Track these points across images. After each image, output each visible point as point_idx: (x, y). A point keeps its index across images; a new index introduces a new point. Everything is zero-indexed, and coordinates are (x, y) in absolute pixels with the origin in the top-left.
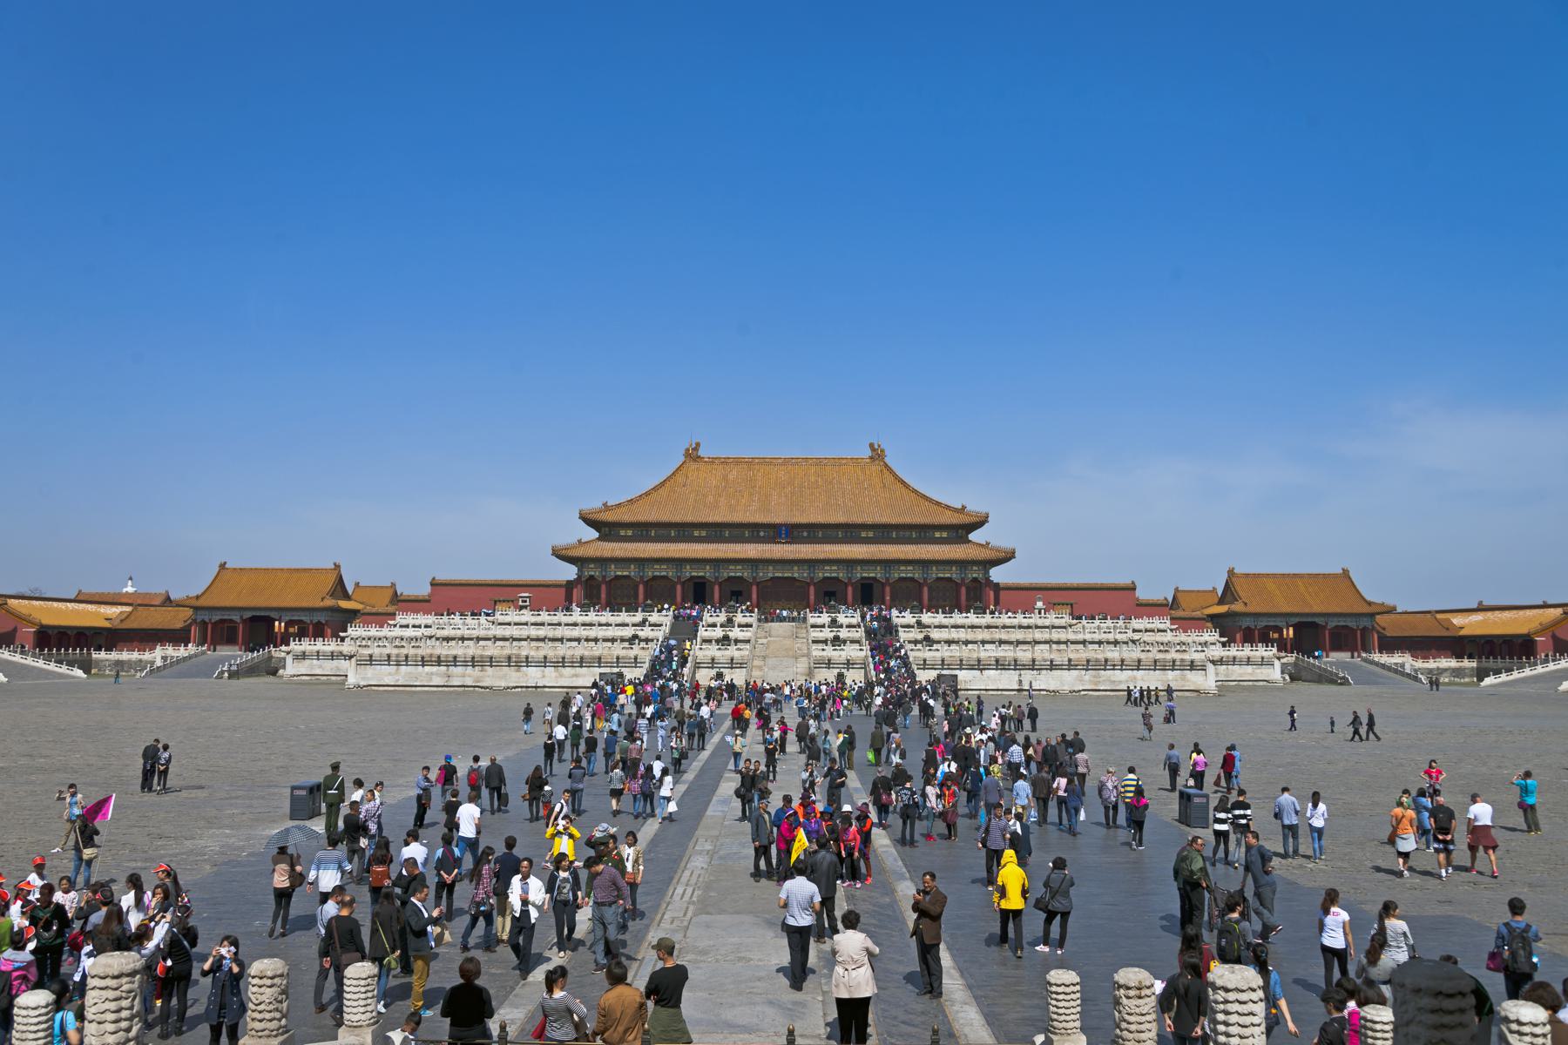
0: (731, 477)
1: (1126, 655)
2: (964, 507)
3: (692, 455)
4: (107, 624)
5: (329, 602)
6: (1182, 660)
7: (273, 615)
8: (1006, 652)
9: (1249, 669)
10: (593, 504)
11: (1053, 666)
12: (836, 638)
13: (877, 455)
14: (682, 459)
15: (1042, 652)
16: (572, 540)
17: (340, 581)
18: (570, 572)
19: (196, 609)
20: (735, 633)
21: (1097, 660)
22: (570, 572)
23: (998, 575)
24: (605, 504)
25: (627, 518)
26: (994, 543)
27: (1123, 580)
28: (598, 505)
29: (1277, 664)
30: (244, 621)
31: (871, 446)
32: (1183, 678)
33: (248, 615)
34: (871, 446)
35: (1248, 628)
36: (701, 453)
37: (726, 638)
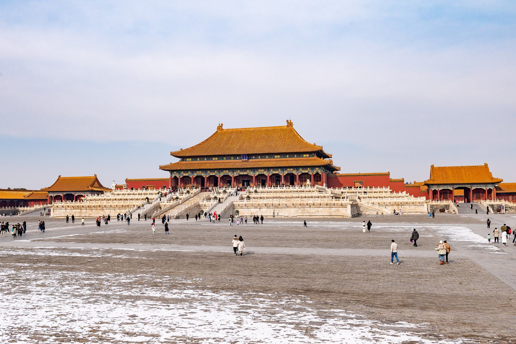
0: (233, 137)
1: (315, 202)
3: (220, 127)
4: (23, 198)
5: (90, 188)
6: (337, 204)
7: (73, 193)
8: (270, 202)
9: (413, 207)
10: (177, 149)
11: (287, 206)
15: (283, 202)
17: (97, 180)
18: (167, 175)
19: (49, 192)
21: (303, 204)
22: (167, 175)
25: (188, 155)
27: (384, 171)
29: (425, 205)
30: (64, 196)
31: (287, 121)
32: (338, 211)
33: (65, 193)
34: (287, 121)
35: (435, 190)
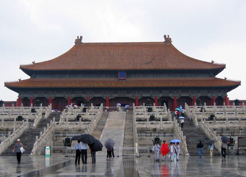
2: (213, 62)
3: (79, 41)
10: (28, 62)
12: (152, 118)
13: (168, 40)
14: (74, 44)
16: (17, 80)
20: (87, 116)
22: (13, 96)
23: (232, 95)
24: (34, 63)
26: (228, 79)
28: (30, 63)
31: (165, 36)
36: (83, 41)
37: (78, 118)
